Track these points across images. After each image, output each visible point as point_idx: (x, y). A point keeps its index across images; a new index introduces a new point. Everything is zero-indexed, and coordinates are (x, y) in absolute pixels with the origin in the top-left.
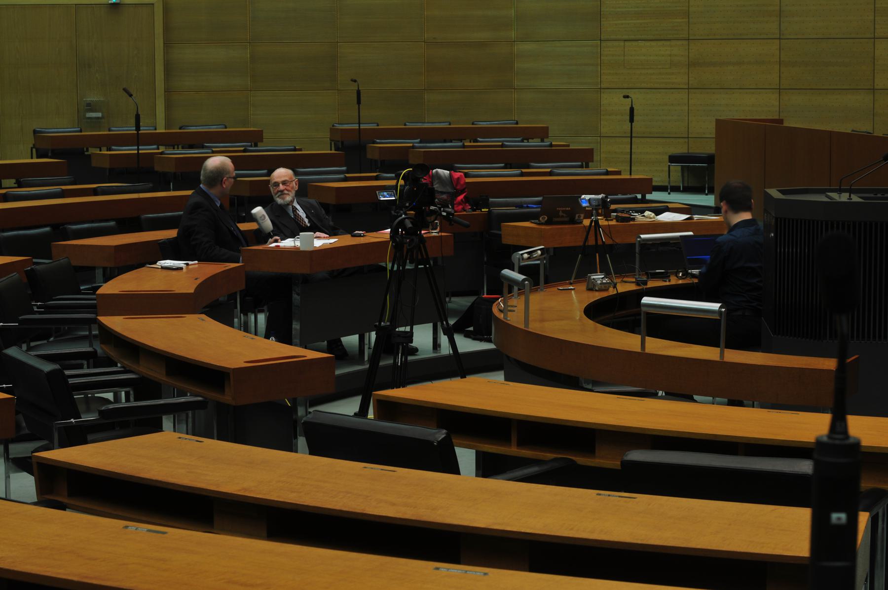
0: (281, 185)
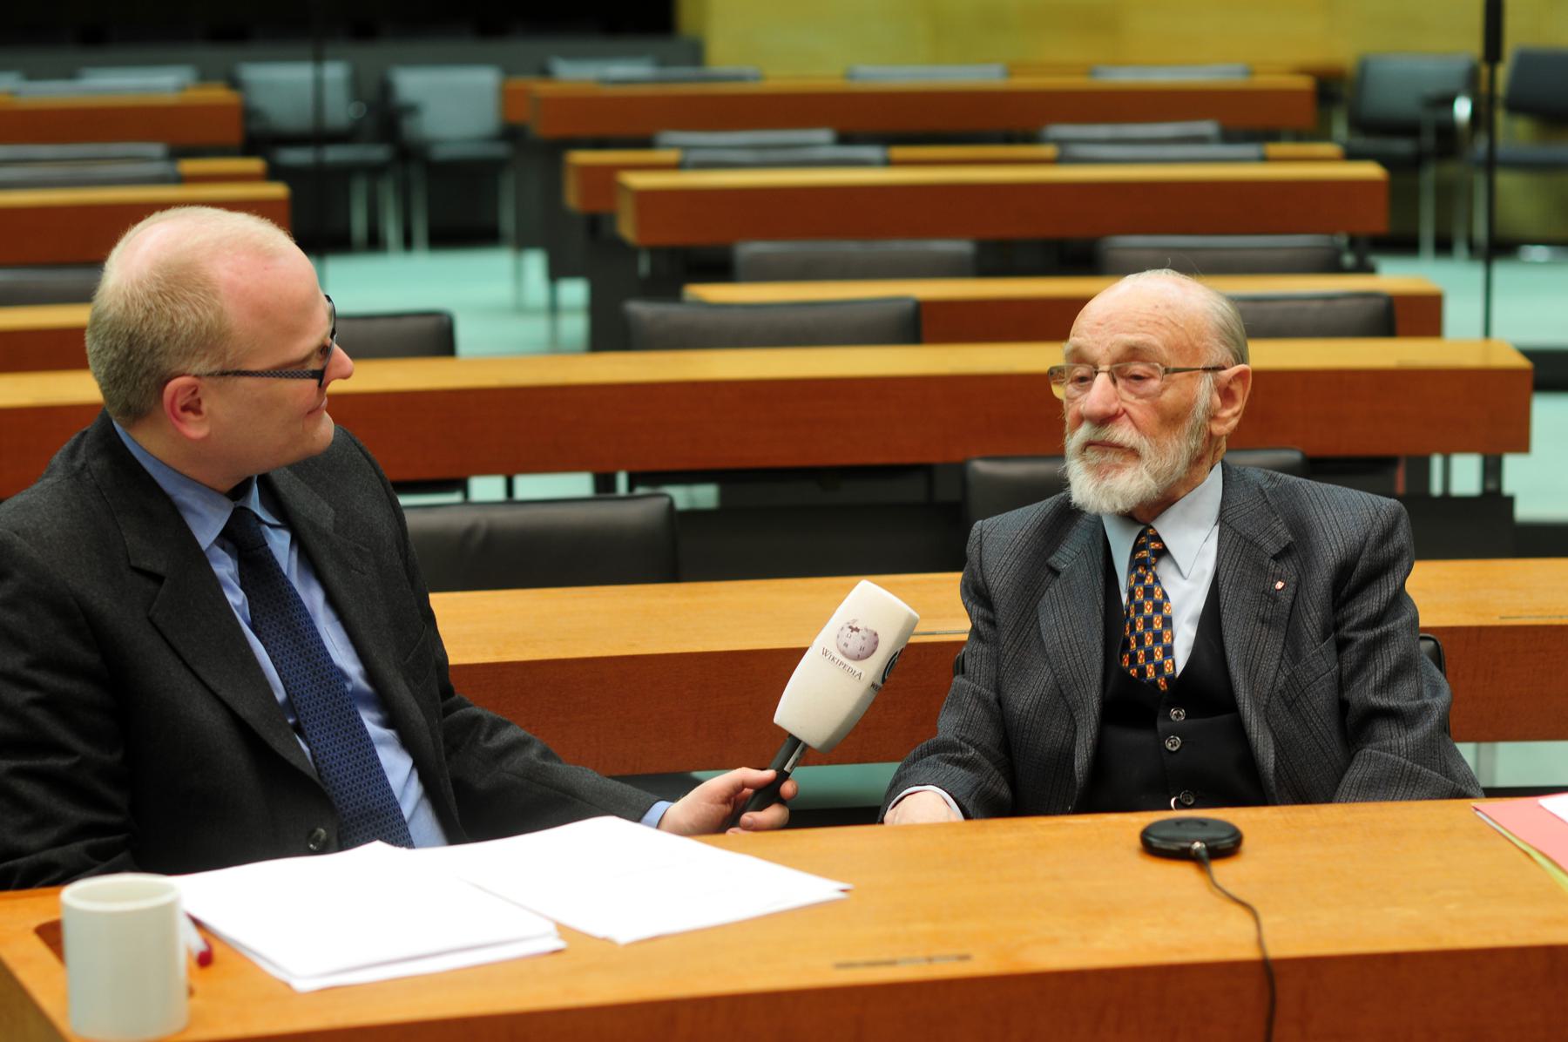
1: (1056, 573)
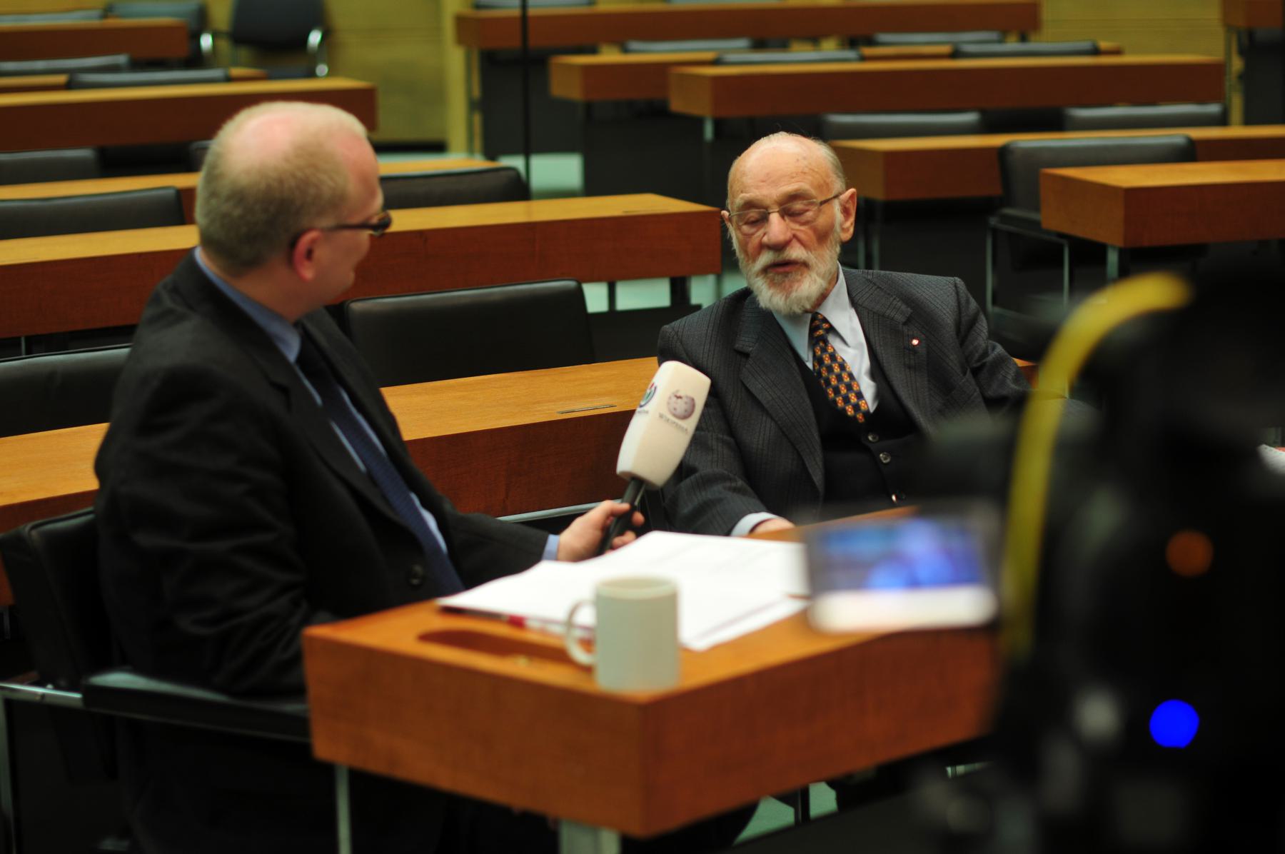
0: (775, 218)
1: (746, 355)
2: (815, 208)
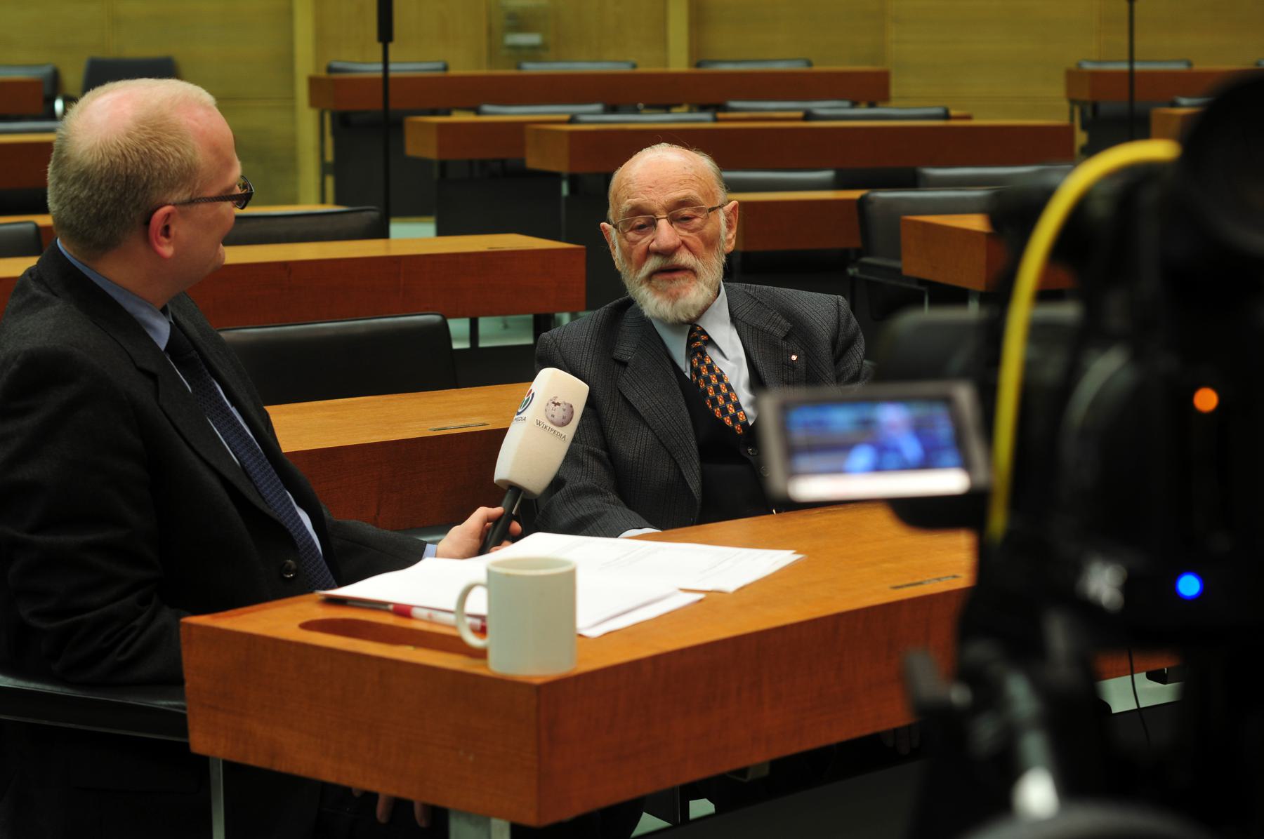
0: (663, 224)
1: (624, 364)
2: (703, 216)
